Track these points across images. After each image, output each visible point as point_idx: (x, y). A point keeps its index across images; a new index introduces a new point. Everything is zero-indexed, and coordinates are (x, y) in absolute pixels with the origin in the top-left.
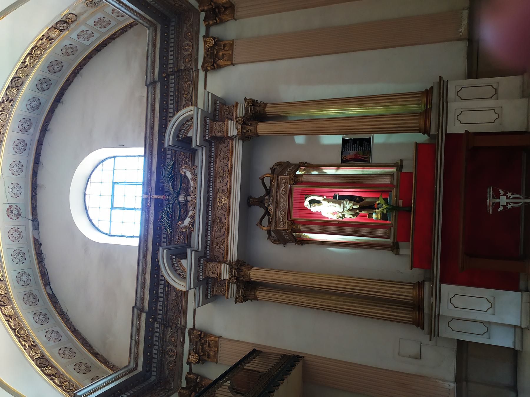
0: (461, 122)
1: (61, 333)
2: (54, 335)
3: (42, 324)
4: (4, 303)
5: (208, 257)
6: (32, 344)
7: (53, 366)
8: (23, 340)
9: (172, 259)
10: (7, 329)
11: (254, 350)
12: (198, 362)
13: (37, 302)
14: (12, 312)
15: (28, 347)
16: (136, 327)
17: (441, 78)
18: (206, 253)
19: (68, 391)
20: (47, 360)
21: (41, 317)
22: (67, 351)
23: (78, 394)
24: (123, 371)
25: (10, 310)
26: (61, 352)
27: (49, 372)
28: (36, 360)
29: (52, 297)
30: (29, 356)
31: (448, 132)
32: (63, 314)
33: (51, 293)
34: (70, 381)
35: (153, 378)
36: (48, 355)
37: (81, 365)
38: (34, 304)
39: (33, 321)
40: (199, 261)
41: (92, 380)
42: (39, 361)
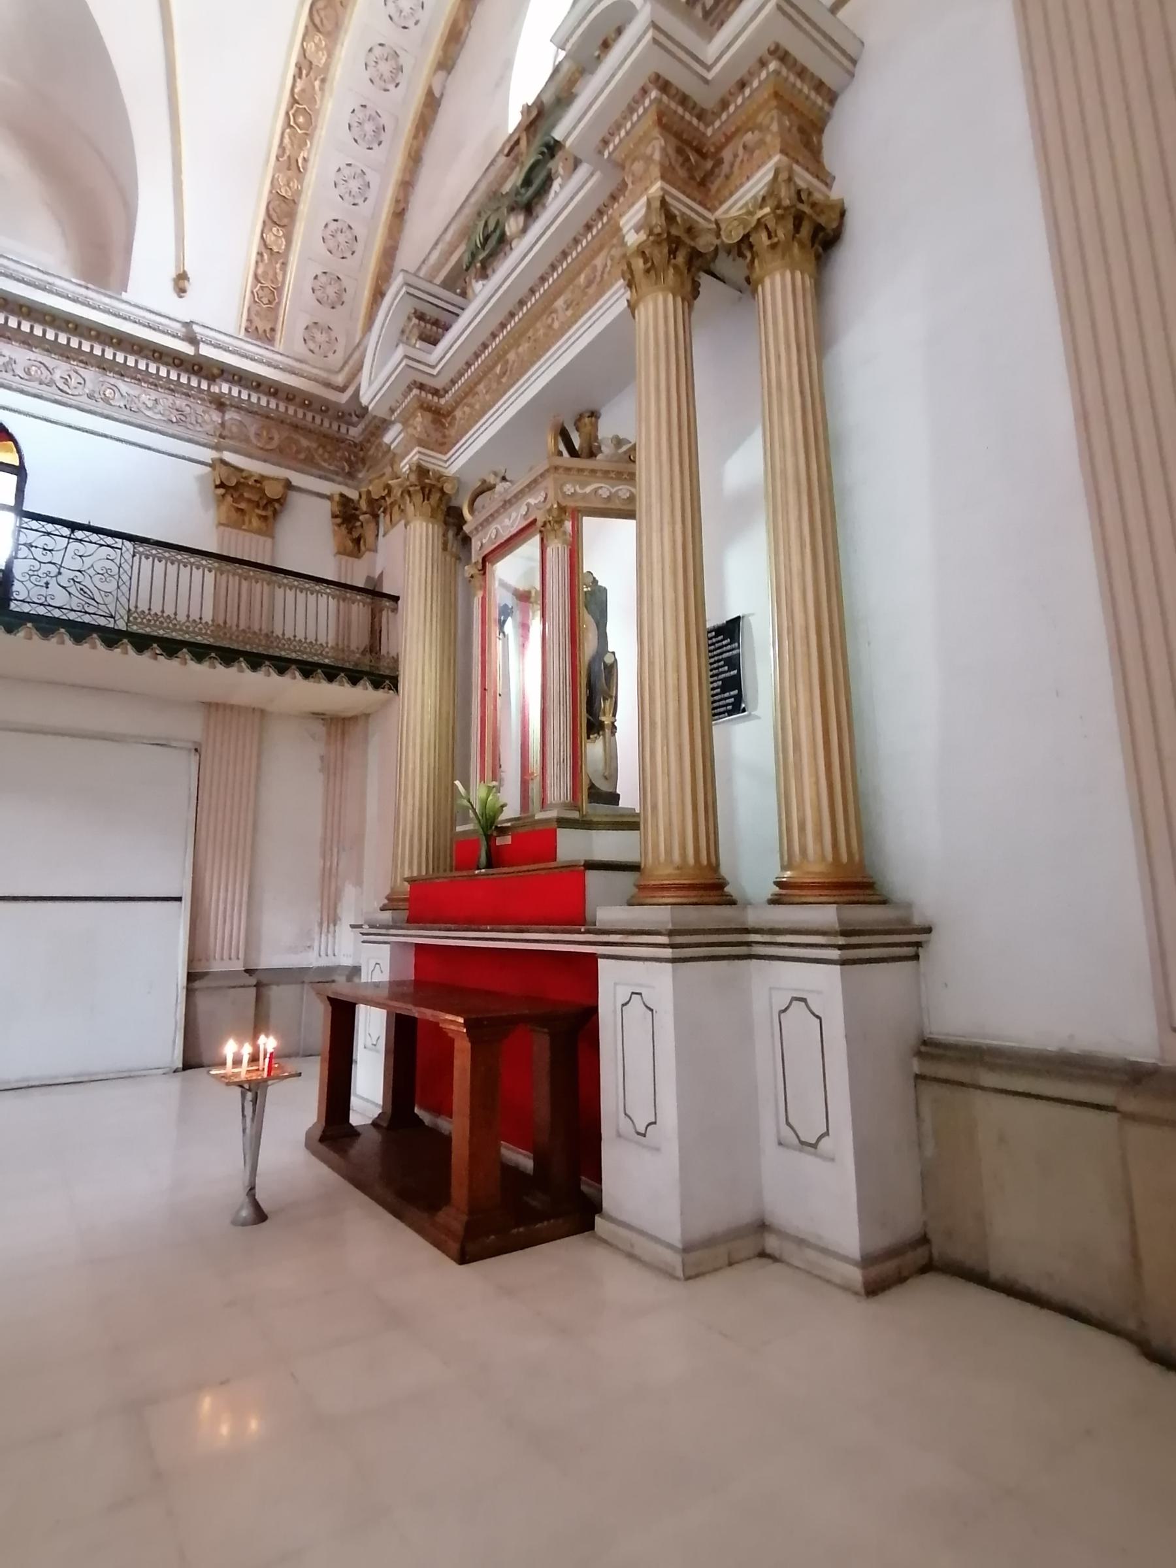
0: (784, 1011)
1: (372, 194)
2: (354, 185)
3: (356, 141)
4: (322, 21)
6: (297, 161)
8: (290, 138)
10: (282, 86)
13: (391, 87)
14: (321, 59)
15: (285, 157)
17: (928, 930)
19: (257, 299)
20: (291, 215)
21: (369, 127)
22: (343, 235)
25: (322, 50)
26: (333, 226)
27: (270, 238)
29: (432, 103)
30: (273, 177)
31: (601, 963)
32: (415, 159)
33: (437, 94)
34: (279, 290)
36: (304, 208)
37: (333, 283)
38: (382, 83)
39: (346, 117)
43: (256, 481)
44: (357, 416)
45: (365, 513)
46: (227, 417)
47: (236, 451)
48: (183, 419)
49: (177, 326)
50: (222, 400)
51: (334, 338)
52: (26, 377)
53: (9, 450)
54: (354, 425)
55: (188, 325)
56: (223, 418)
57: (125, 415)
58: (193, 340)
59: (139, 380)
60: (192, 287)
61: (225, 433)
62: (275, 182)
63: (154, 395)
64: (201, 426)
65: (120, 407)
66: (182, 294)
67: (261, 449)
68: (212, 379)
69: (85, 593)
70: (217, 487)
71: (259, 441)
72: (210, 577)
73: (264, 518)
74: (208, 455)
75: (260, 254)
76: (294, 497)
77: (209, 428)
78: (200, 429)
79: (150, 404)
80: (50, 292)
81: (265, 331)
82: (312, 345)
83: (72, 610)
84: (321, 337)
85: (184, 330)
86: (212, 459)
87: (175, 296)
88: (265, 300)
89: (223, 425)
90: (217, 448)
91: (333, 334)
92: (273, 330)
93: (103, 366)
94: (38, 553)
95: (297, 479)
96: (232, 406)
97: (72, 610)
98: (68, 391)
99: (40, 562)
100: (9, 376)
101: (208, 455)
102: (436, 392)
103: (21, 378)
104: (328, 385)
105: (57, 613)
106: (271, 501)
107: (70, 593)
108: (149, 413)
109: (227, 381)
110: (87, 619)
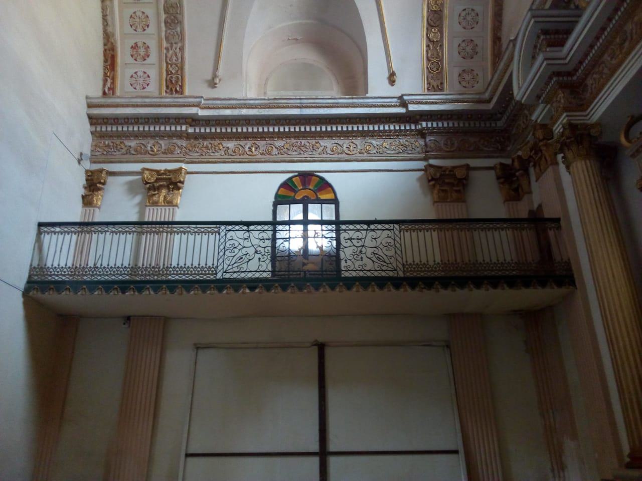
5: (575, 78)
9: (539, 37)
11: (558, 220)
16: (505, 64)
18: (576, 70)
26: (463, 14)
27: (431, 35)
34: (441, 61)
35: (500, 124)
36: (446, 12)
40: (550, 78)
41: (463, 71)
42: (432, 15)
43: (450, 171)
44: (501, 113)
45: (519, 170)
46: (427, 140)
47: (436, 158)
48: (406, 149)
49: (395, 100)
50: (424, 131)
51: (475, 75)
52: (332, 153)
53: (329, 193)
54: (500, 119)
55: (401, 98)
56: (425, 141)
57: (377, 156)
58: (404, 104)
59: (381, 136)
60: (398, 79)
61: (428, 149)
62: (430, 5)
63: (389, 141)
64: (415, 150)
65: (375, 153)
66: (394, 84)
67: (449, 152)
68: (416, 122)
69: (380, 259)
70: (429, 181)
71: (447, 148)
72: (435, 234)
73: (458, 191)
74: (421, 164)
75: (428, 46)
76: (473, 174)
77: (419, 149)
78: (415, 152)
79: (388, 147)
80: (338, 107)
81: (438, 86)
82: (464, 84)
83: (376, 271)
84: (468, 77)
85: (399, 101)
86: (425, 166)
87: (390, 86)
88: (434, 69)
89: (426, 145)
90: (425, 159)
91: (475, 73)
92: (442, 84)
93: (364, 134)
94: (355, 242)
95: (473, 163)
96: (429, 133)
97: (376, 271)
98: (351, 153)
99: (357, 247)
100: (325, 155)
101: (421, 164)
102: (569, 74)
103: (330, 154)
104: (480, 101)
105: (369, 274)
106: (460, 180)
107: (373, 261)
108: (388, 152)
109: (424, 120)
110: (384, 274)
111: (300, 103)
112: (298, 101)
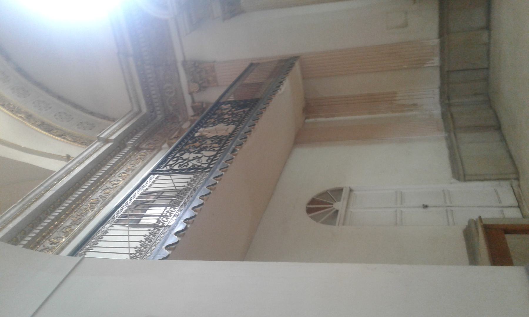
7: (57, 129)
12: (200, 90)
23: (102, 136)
24: (130, 115)
27: (58, 133)
28: (39, 126)
68: (125, 146)
89: (148, 149)
109: (128, 141)
111: (46, 188)
112: (42, 188)
